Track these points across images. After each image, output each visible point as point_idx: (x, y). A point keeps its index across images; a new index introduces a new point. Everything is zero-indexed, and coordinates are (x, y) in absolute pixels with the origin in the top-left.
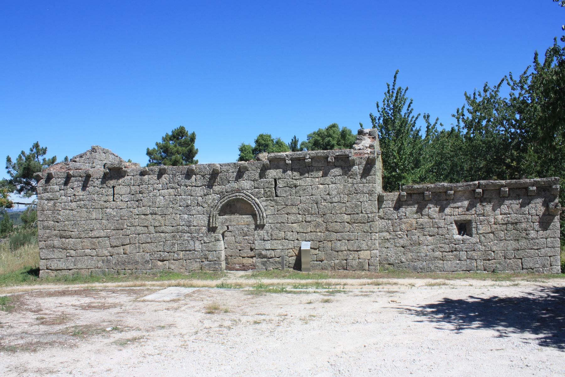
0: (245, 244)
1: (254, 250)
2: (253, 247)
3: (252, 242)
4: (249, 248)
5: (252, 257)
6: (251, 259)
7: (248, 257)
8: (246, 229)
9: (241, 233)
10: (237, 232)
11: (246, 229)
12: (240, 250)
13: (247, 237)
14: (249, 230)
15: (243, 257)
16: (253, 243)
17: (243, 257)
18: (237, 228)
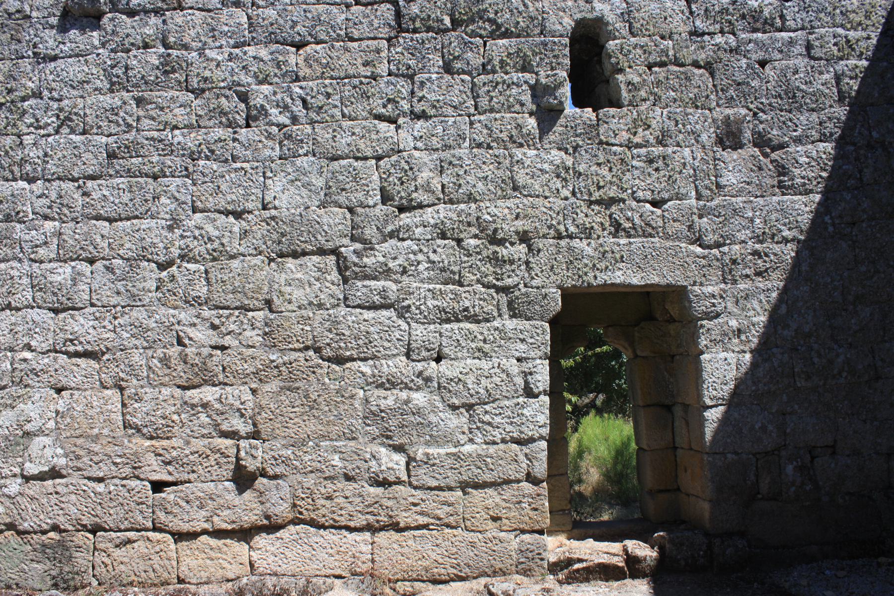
0: (199, 444)
1: (261, 481)
2: (251, 465)
3: (243, 428)
4: (227, 471)
5: (245, 534)
6: (240, 548)
7: (218, 534)
8: (201, 335)
9: (165, 361)
10: (137, 358)
11: (201, 335)
12: (158, 486)
13: (209, 394)
14: (228, 341)
15: (180, 536)
16: (255, 435)
17: (180, 536)
18: (141, 330)
